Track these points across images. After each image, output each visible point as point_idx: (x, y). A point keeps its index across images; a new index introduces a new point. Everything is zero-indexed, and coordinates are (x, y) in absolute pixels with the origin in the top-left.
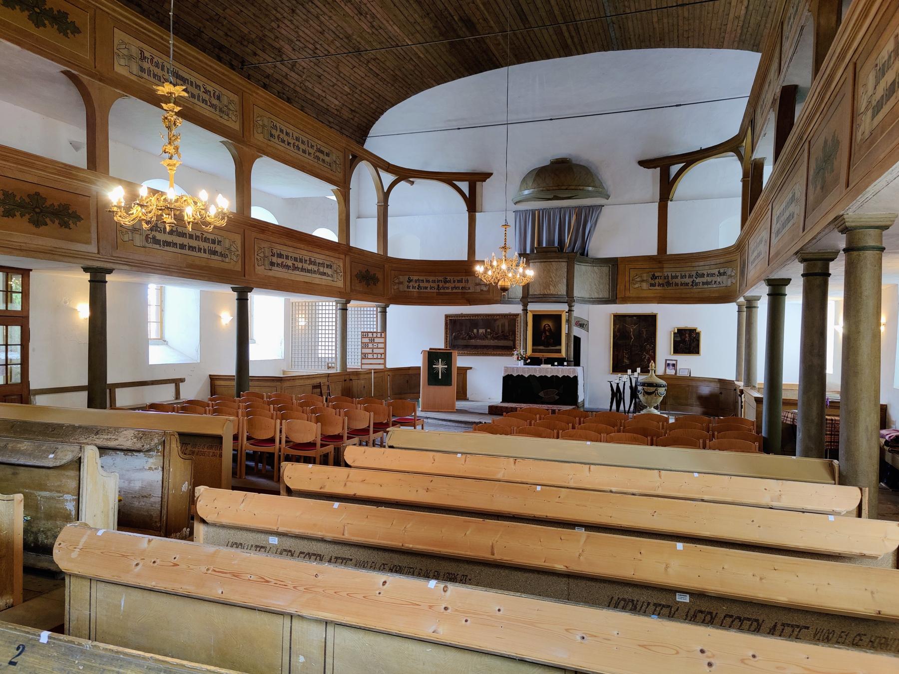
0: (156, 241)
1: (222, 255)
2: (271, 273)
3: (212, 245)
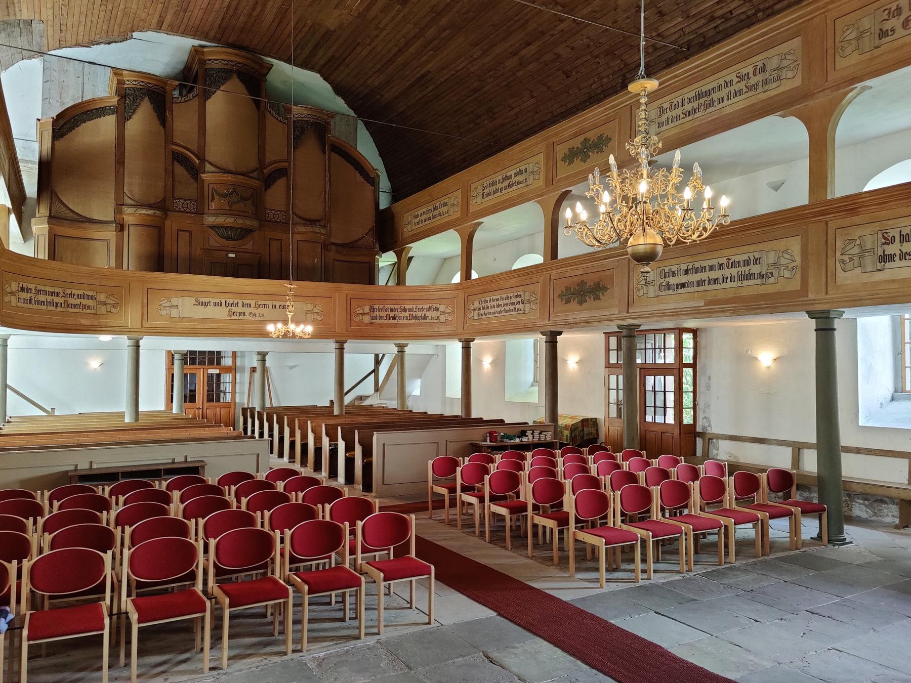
0: (669, 287)
1: (761, 276)
2: (879, 276)
3: (743, 269)
